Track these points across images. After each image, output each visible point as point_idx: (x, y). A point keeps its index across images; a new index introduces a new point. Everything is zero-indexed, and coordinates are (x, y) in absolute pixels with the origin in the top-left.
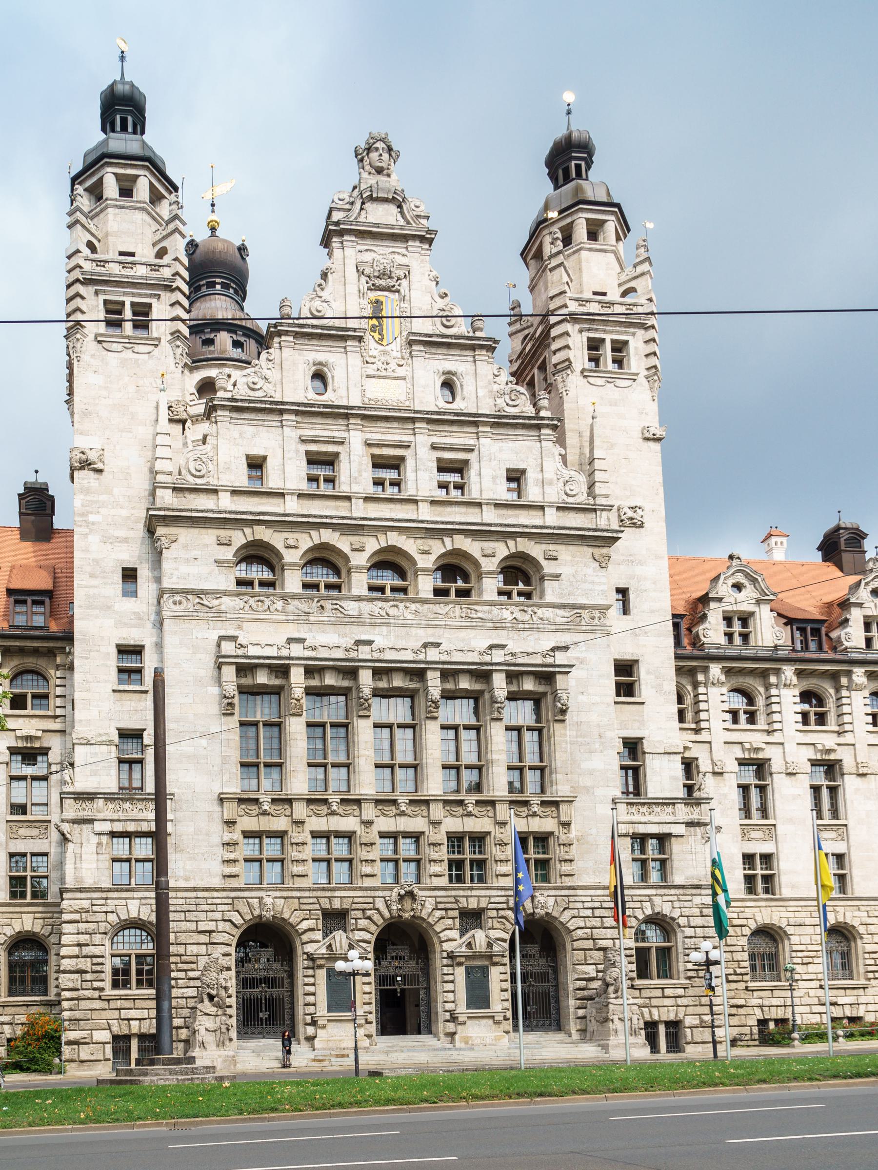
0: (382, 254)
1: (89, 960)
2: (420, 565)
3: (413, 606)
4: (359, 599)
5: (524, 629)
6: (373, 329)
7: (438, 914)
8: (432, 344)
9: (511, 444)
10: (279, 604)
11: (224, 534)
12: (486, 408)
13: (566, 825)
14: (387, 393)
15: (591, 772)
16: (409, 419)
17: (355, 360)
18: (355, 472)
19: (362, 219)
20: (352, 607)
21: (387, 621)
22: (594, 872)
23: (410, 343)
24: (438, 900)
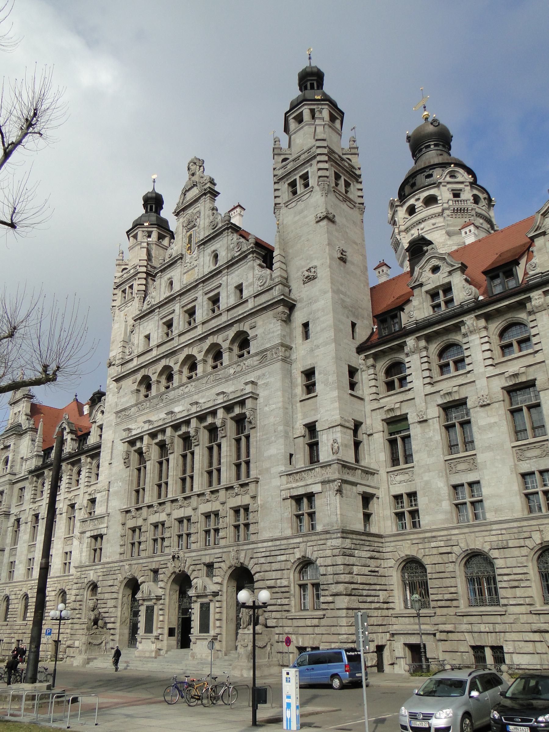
1: (78, 603)
3: (193, 384)
5: (239, 376)
7: (192, 567)
9: (236, 273)
13: (254, 497)
15: (269, 457)
18: (180, 324)
22: (269, 529)
23: (199, 246)
24: (194, 558)
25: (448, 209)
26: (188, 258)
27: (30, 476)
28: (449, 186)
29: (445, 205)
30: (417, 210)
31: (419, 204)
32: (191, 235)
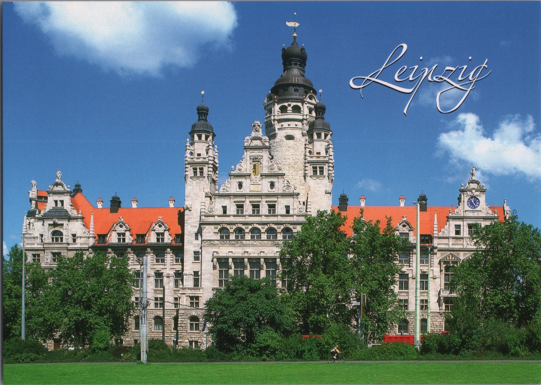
0: (256, 153)
2: (262, 231)
4: (247, 240)
6: (254, 172)
8: (267, 176)
10: (228, 242)
11: (216, 226)
12: (280, 192)
14: (255, 189)
16: (260, 196)
17: (248, 181)
18: (248, 209)
19: (251, 145)
20: (244, 242)
21: (253, 246)
23: (261, 176)
25: (306, 120)
26: (253, 176)
27: (90, 249)
28: (308, 105)
29: (305, 117)
30: (288, 112)
31: (290, 108)
32: (255, 165)
